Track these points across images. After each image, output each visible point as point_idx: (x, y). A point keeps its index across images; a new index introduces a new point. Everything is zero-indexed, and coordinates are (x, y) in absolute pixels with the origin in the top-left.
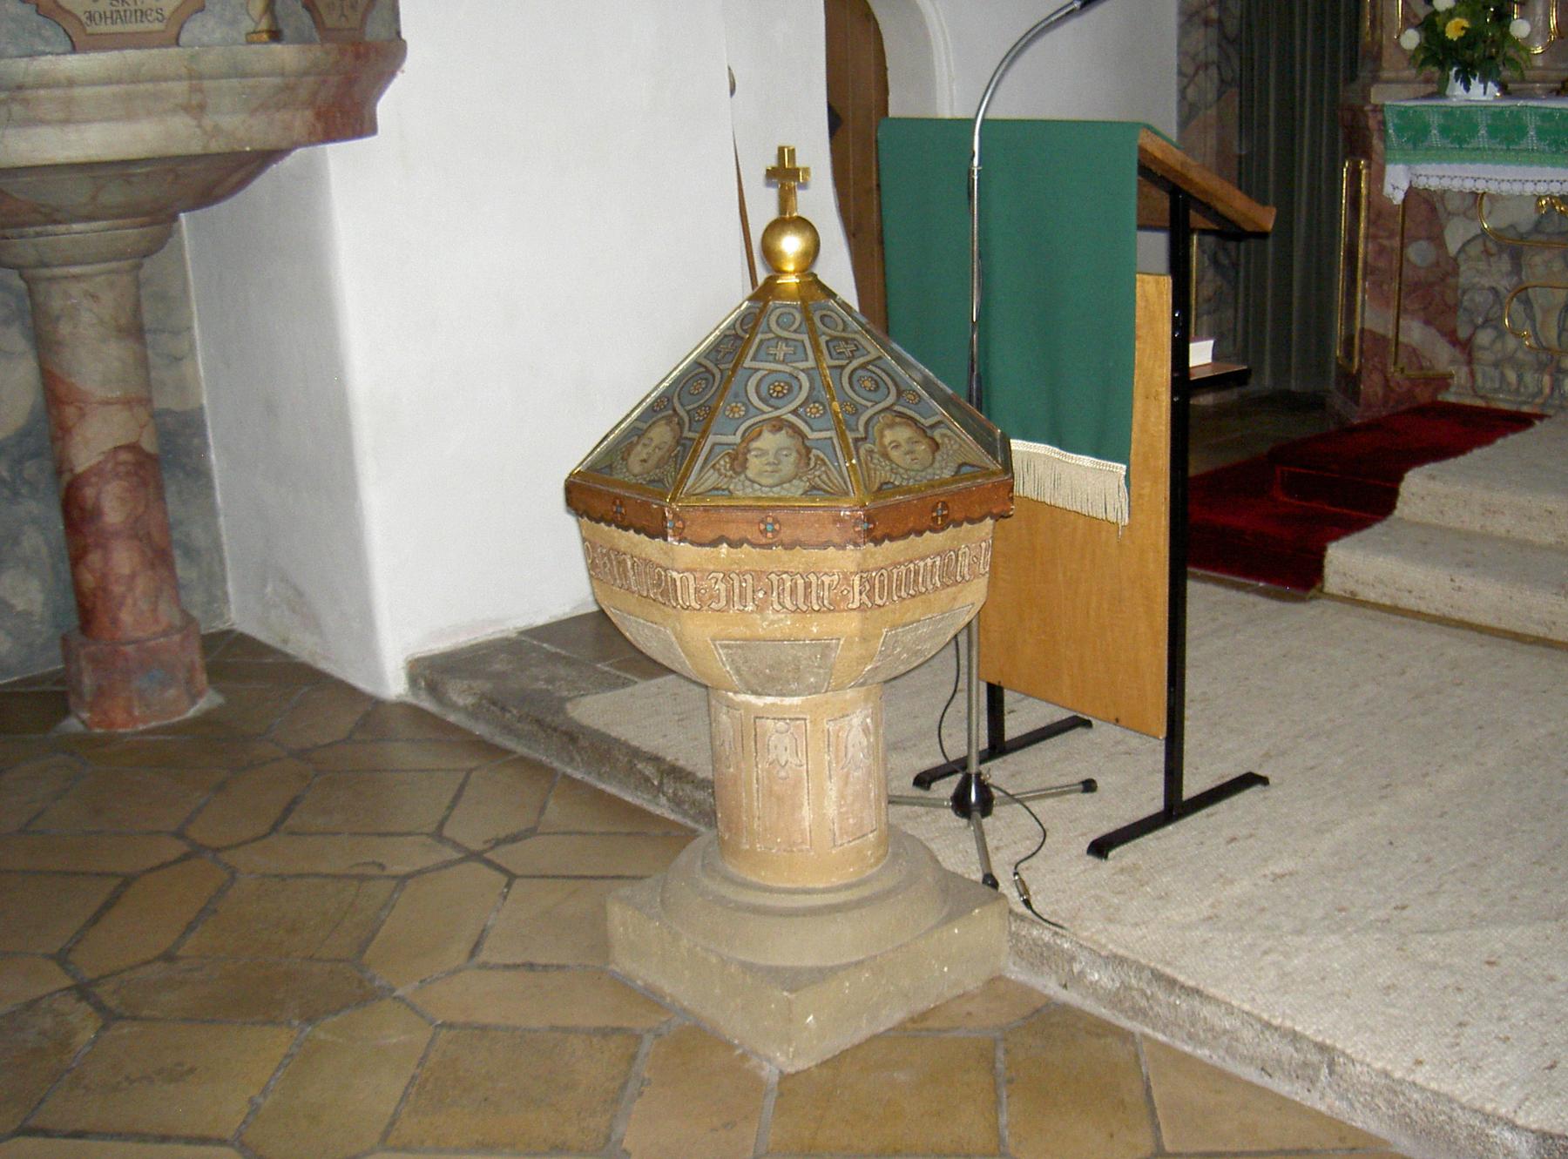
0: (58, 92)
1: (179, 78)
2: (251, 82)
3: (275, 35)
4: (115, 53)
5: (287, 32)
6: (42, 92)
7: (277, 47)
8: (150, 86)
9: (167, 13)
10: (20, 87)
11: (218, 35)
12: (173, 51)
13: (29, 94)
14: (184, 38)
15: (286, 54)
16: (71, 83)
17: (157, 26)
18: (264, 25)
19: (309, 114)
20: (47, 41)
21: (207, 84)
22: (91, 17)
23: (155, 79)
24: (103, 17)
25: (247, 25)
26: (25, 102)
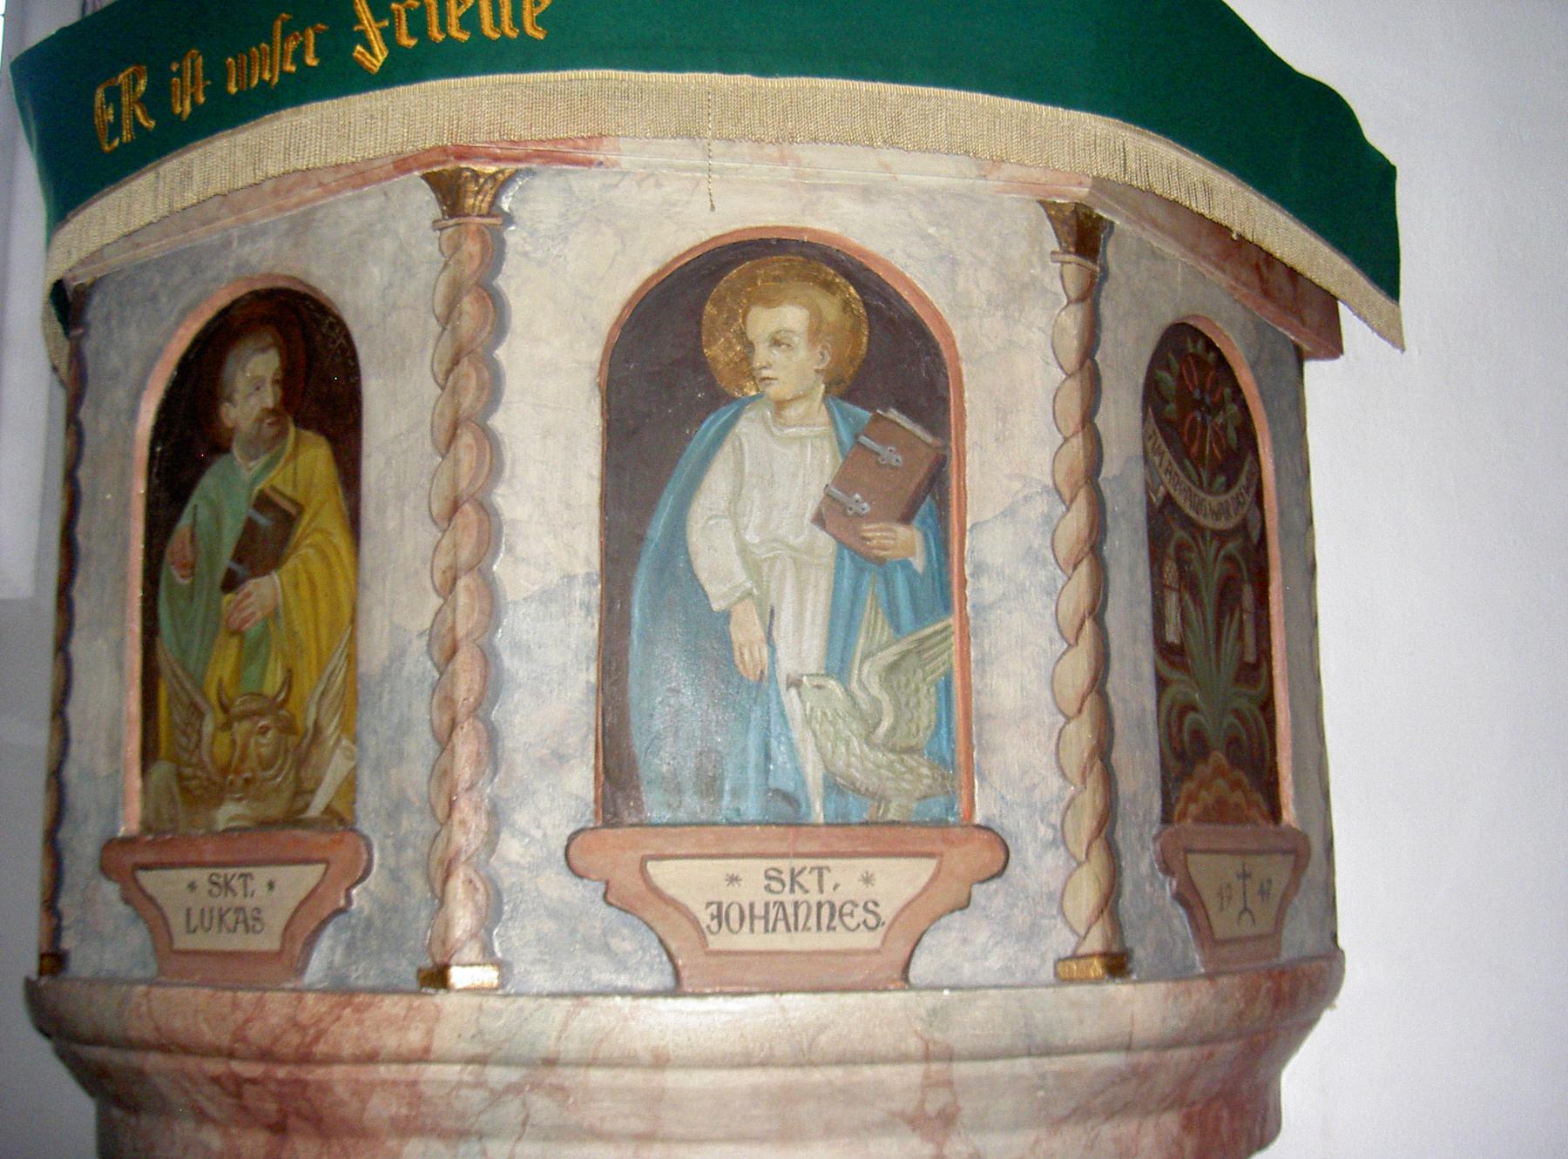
0: (630, 1077)
1: (903, 1058)
2: (1057, 1064)
3: (1117, 965)
4: (762, 1002)
5: (1142, 954)
6: (597, 1076)
7: (1119, 990)
8: (836, 1074)
9: (887, 912)
10: (551, 1062)
11: (994, 962)
12: (893, 1000)
13: (567, 1076)
14: (921, 968)
15: (1140, 1005)
16: (660, 1062)
17: (865, 940)
18: (1095, 943)
19: (1171, 1121)
20: (621, 964)
21: (962, 1070)
22: (721, 916)
23: (843, 1060)
24: (748, 916)
25: (1061, 941)
26: (559, 1091)
